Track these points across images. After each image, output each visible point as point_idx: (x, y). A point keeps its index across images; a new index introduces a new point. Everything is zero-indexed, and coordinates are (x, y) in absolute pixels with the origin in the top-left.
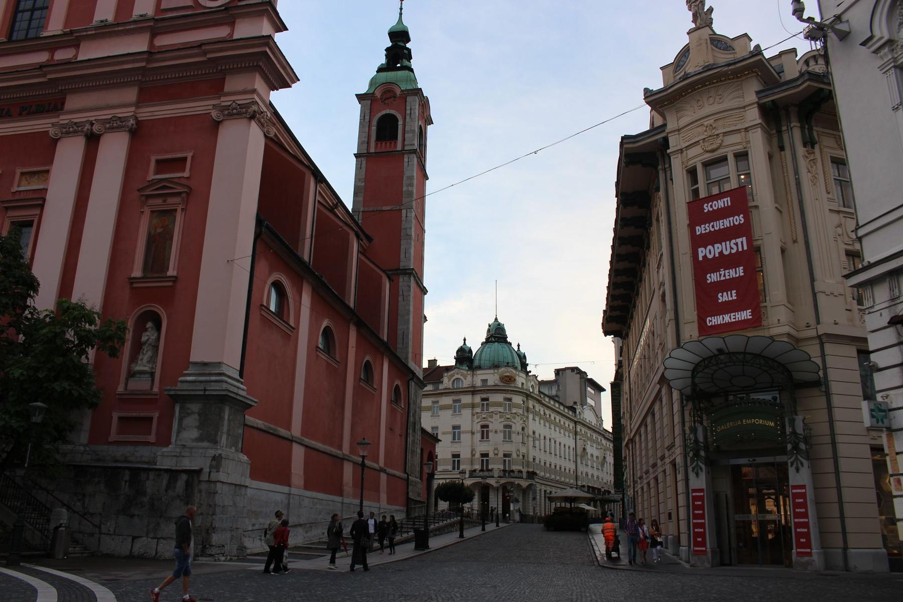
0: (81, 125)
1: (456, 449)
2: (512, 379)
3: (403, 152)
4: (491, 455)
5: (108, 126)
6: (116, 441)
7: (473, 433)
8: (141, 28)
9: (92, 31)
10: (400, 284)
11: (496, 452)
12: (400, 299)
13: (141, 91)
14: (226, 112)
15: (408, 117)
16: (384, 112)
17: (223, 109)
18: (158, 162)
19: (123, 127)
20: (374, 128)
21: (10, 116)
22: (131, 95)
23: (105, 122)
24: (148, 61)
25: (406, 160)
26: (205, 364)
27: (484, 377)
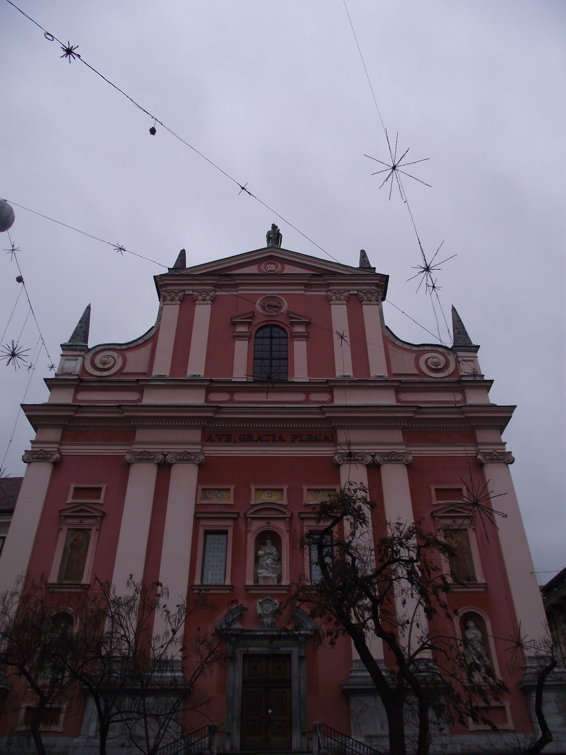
5: (386, 458)
6: (477, 730)
8: (388, 386)
9: (346, 383)
13: (405, 434)
14: (488, 457)
17: (485, 455)
18: (436, 490)
19: (399, 460)
21: (284, 441)
22: (397, 436)
23: (382, 455)
24: (415, 413)
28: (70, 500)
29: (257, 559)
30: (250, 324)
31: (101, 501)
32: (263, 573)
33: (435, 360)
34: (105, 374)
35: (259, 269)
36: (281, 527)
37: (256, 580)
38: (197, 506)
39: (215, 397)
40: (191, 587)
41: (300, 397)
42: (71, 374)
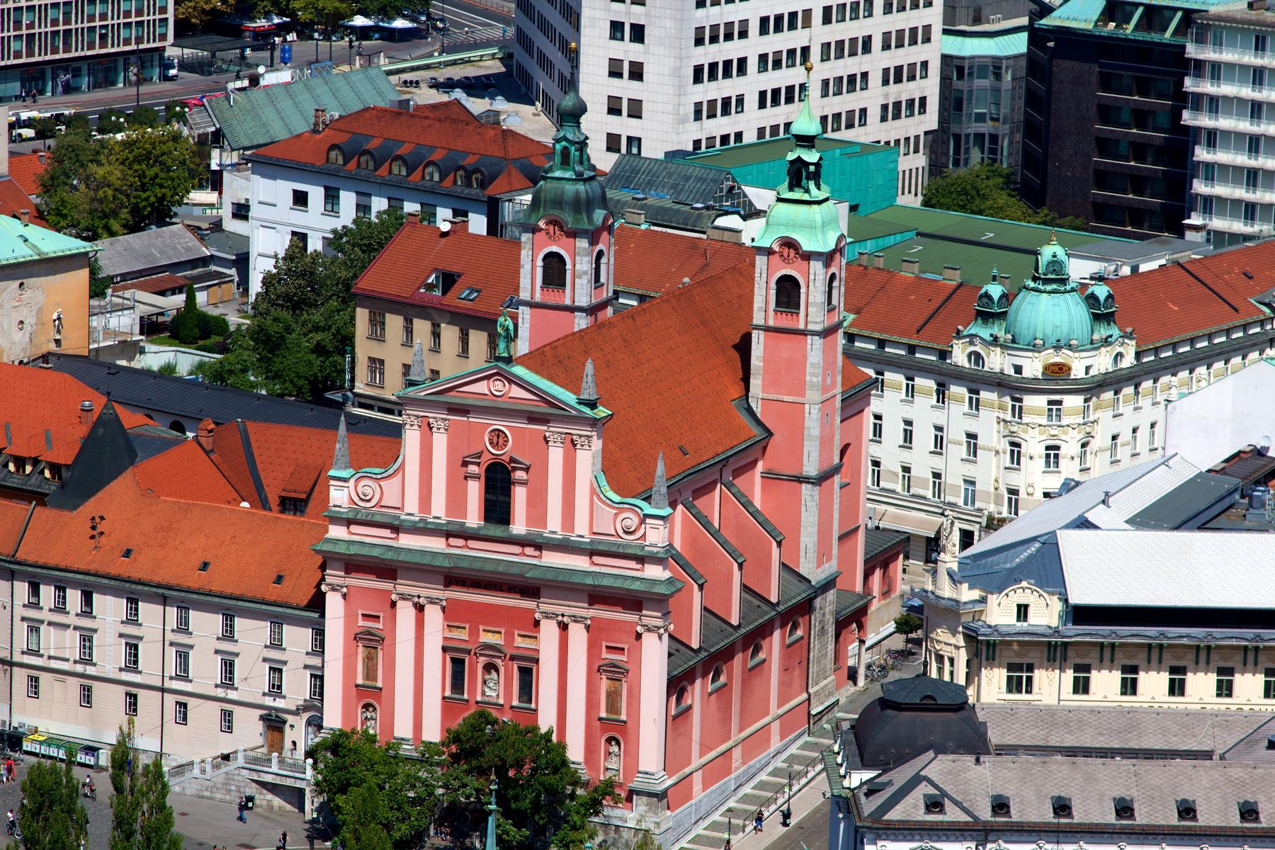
0: (557, 615)
1: (970, 471)
2: (1065, 368)
3: (804, 333)
4: (1022, 495)
7: (997, 452)
10: (803, 492)
11: (1030, 490)
12: (803, 508)
13: (590, 596)
15: (811, 284)
16: (784, 272)
20: (773, 292)
25: (809, 341)
26: (647, 773)
27: (1018, 361)
28: (361, 623)
29: (484, 682)
30: (478, 464)
31: (381, 627)
32: (488, 692)
33: (628, 522)
34: (368, 505)
35: (488, 385)
36: (499, 662)
37: (483, 694)
38: (445, 639)
39: (452, 541)
40: (444, 698)
41: (517, 549)
42: (340, 507)
